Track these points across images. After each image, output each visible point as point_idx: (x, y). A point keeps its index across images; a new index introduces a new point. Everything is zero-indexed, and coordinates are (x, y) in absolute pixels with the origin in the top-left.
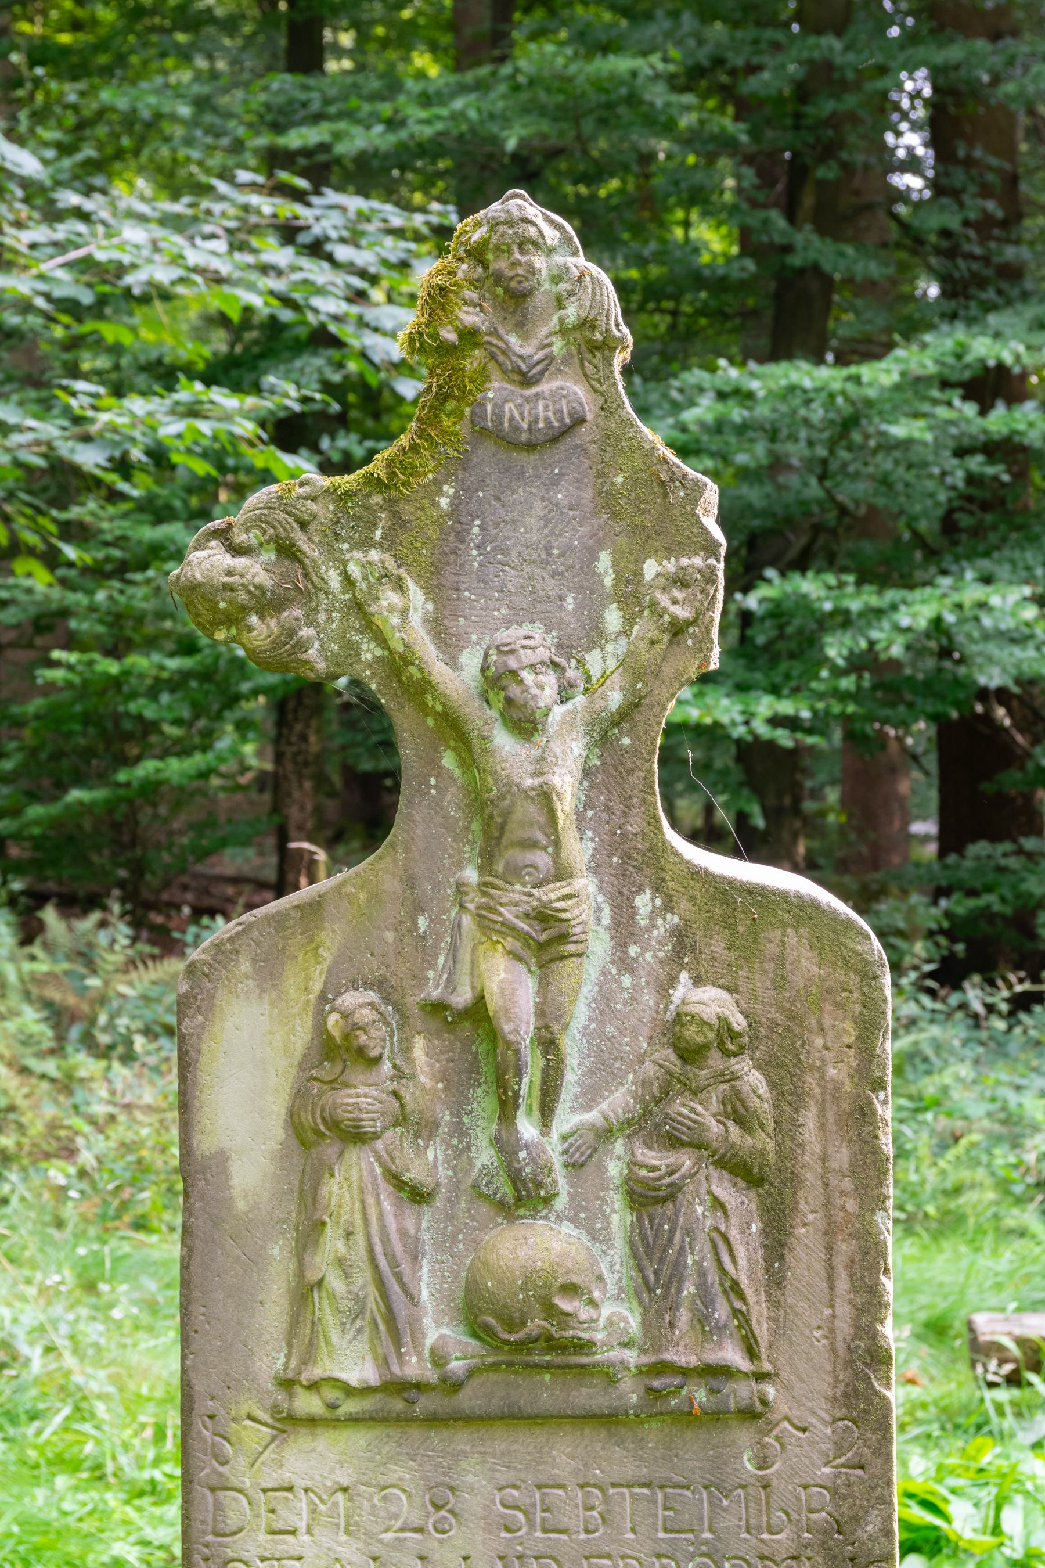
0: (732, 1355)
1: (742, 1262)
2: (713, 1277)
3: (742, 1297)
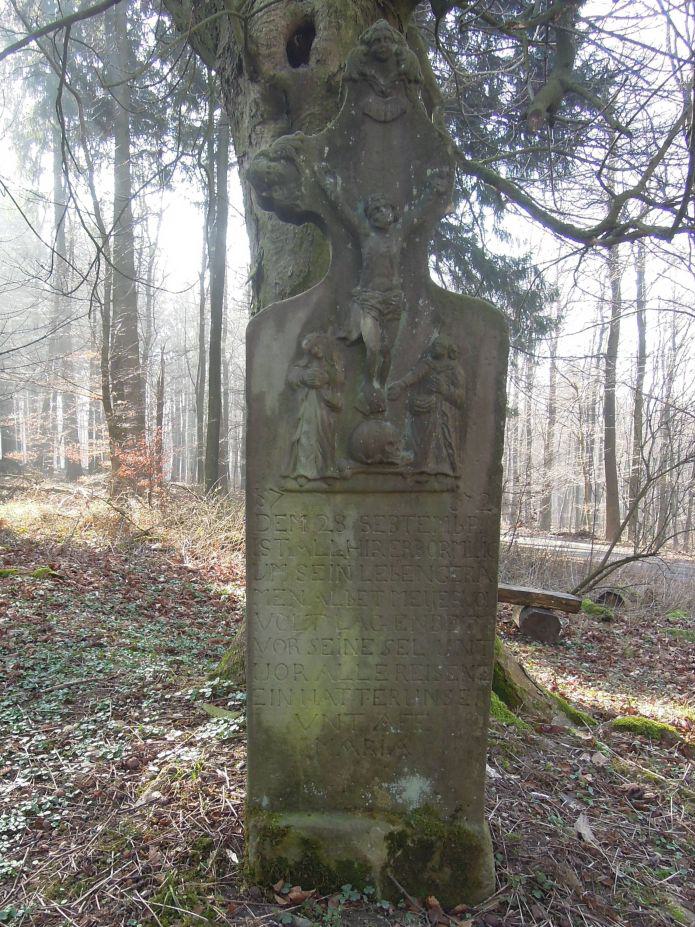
0: (447, 469)
1: (453, 435)
2: (442, 441)
3: (452, 448)
